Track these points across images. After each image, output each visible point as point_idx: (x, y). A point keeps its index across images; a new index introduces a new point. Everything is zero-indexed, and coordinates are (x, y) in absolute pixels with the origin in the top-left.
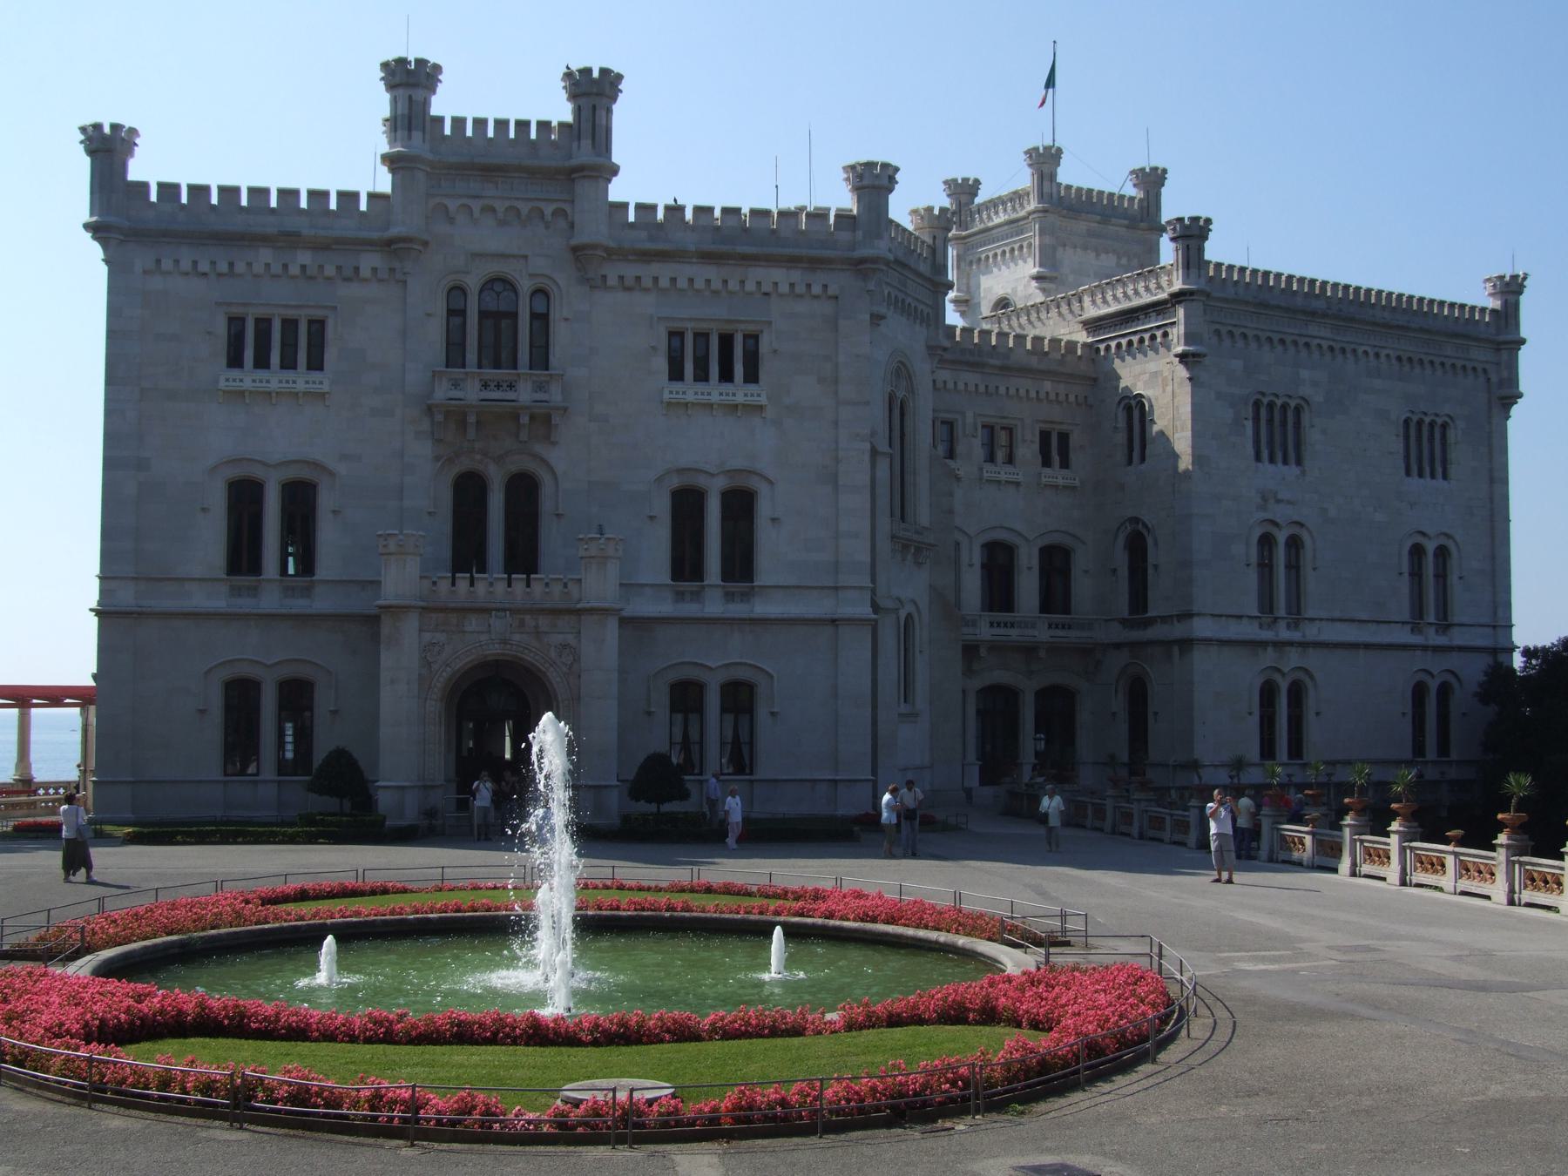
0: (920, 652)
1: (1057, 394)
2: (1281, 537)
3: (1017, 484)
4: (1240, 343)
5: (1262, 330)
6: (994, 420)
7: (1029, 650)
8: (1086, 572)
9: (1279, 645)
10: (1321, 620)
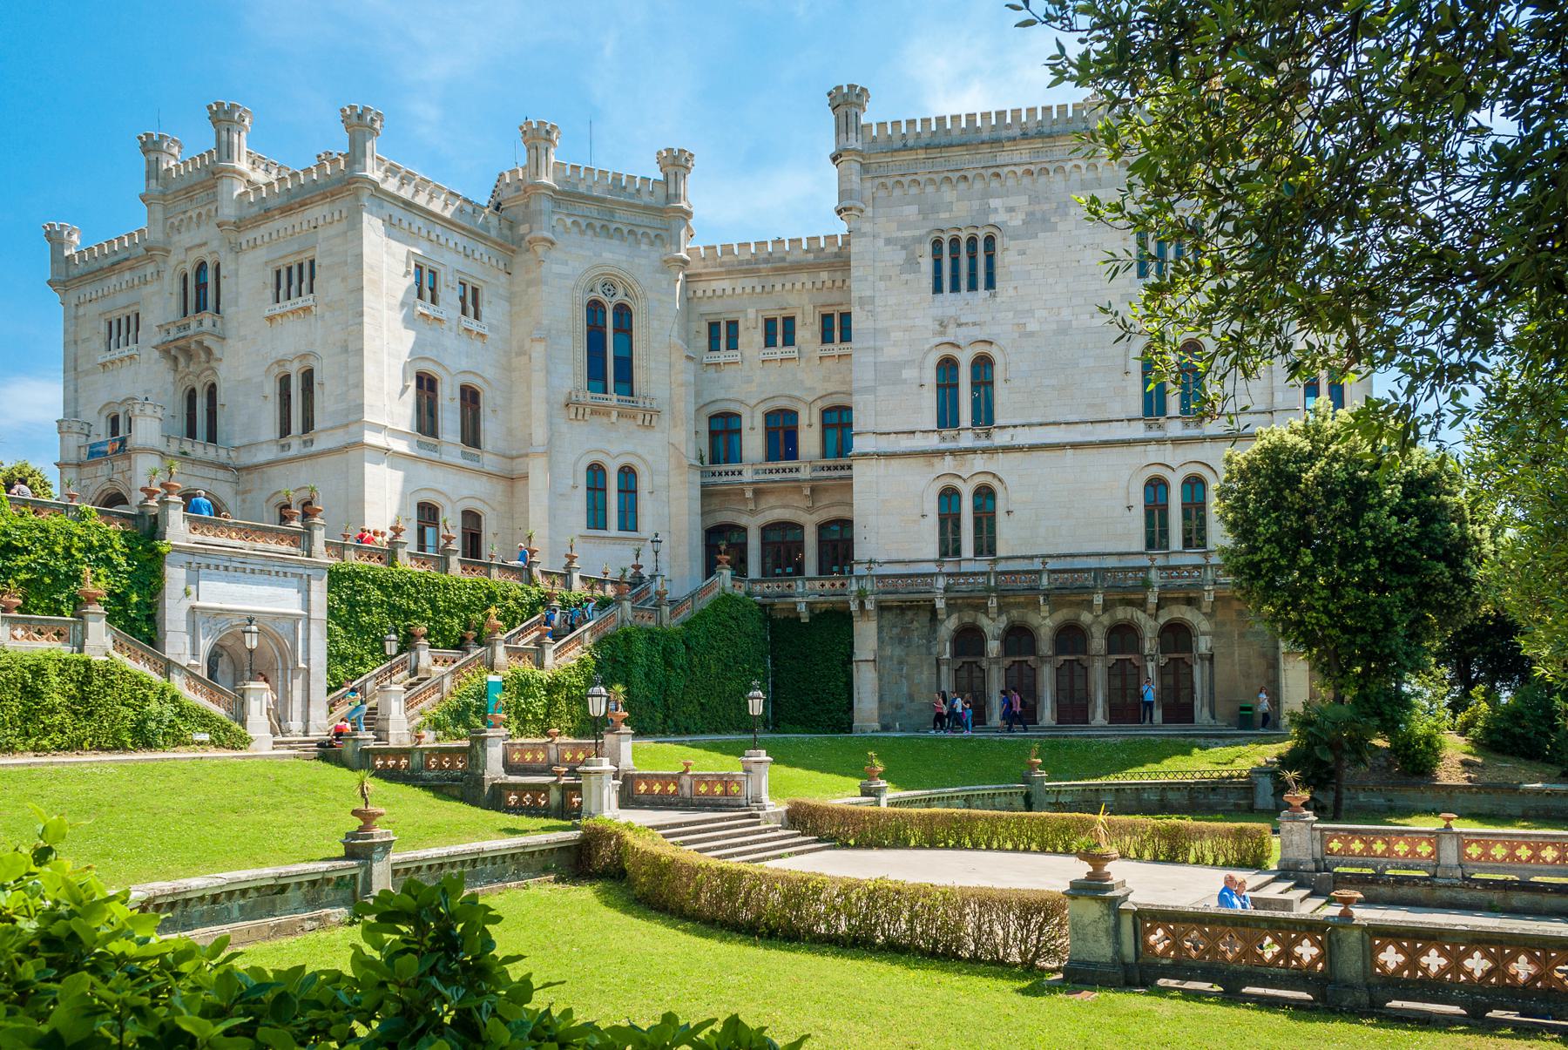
2: (965, 359)
4: (914, 190)
5: (937, 172)
7: (796, 486)
9: (953, 453)
10: (1015, 426)
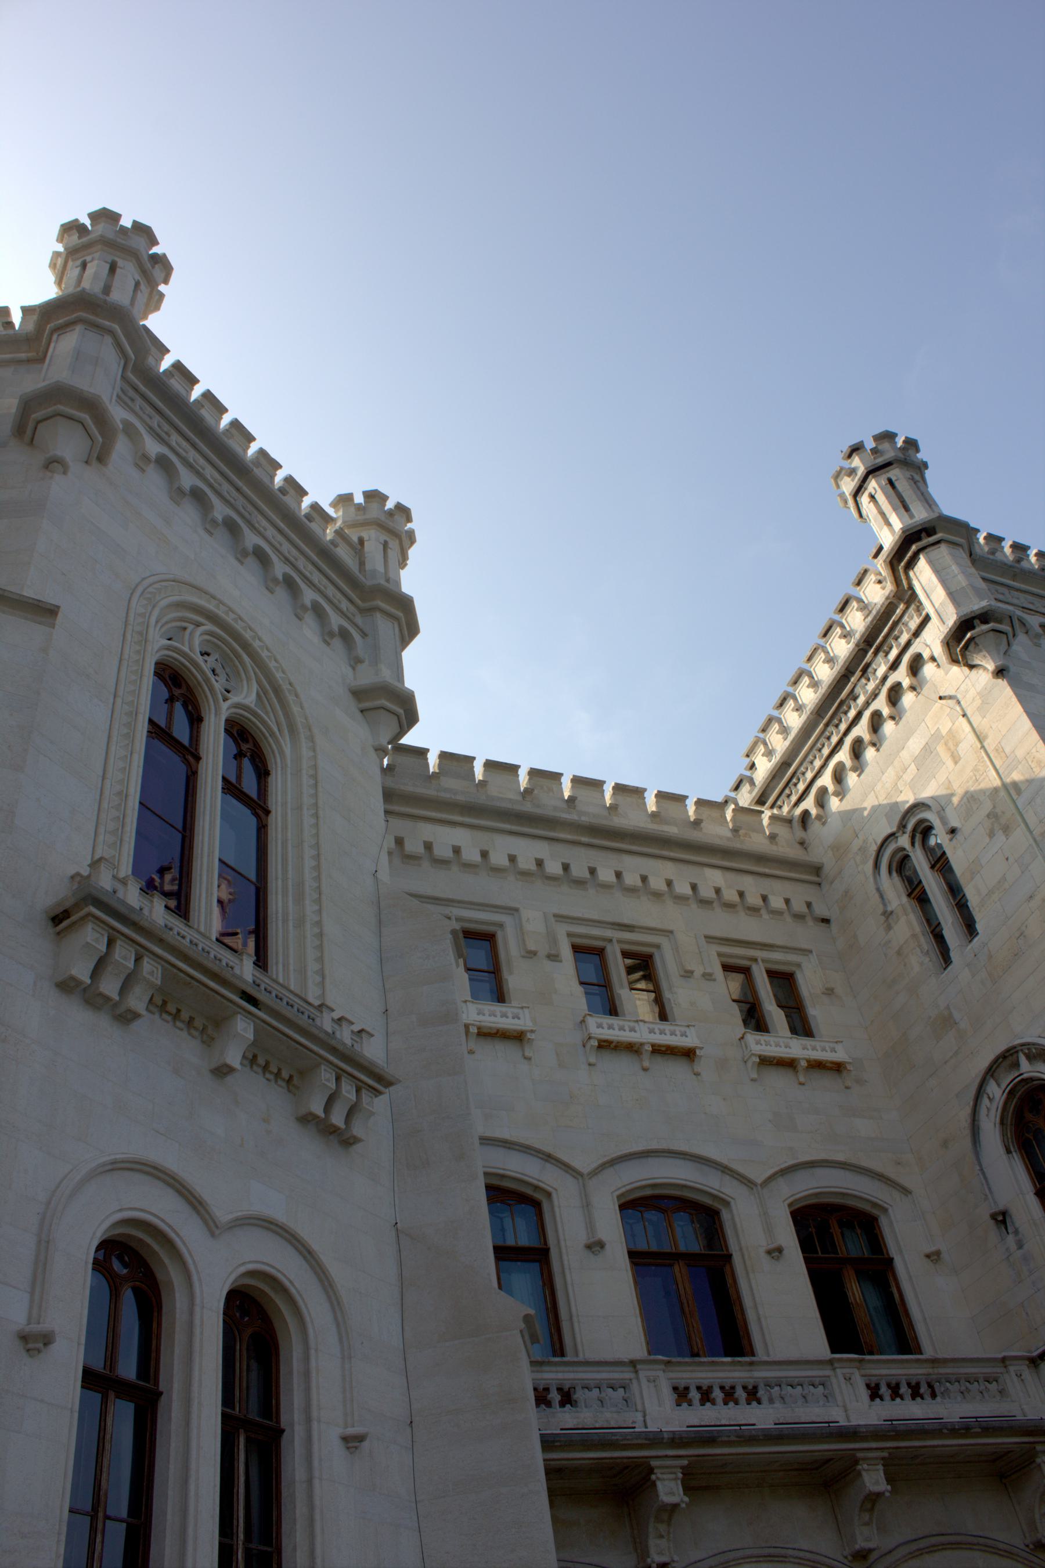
0: (352, 1442)
1: (741, 894)
3: (688, 1054)
6: (609, 933)
8: (934, 1257)
